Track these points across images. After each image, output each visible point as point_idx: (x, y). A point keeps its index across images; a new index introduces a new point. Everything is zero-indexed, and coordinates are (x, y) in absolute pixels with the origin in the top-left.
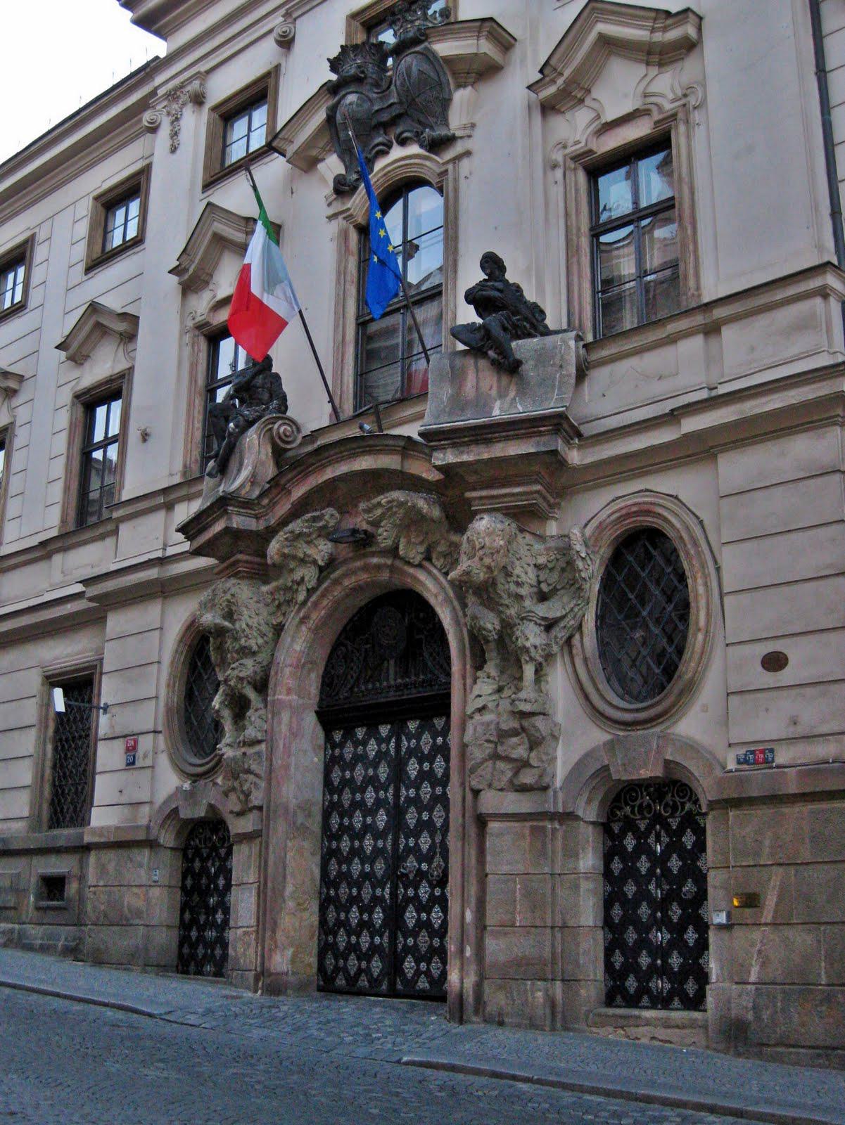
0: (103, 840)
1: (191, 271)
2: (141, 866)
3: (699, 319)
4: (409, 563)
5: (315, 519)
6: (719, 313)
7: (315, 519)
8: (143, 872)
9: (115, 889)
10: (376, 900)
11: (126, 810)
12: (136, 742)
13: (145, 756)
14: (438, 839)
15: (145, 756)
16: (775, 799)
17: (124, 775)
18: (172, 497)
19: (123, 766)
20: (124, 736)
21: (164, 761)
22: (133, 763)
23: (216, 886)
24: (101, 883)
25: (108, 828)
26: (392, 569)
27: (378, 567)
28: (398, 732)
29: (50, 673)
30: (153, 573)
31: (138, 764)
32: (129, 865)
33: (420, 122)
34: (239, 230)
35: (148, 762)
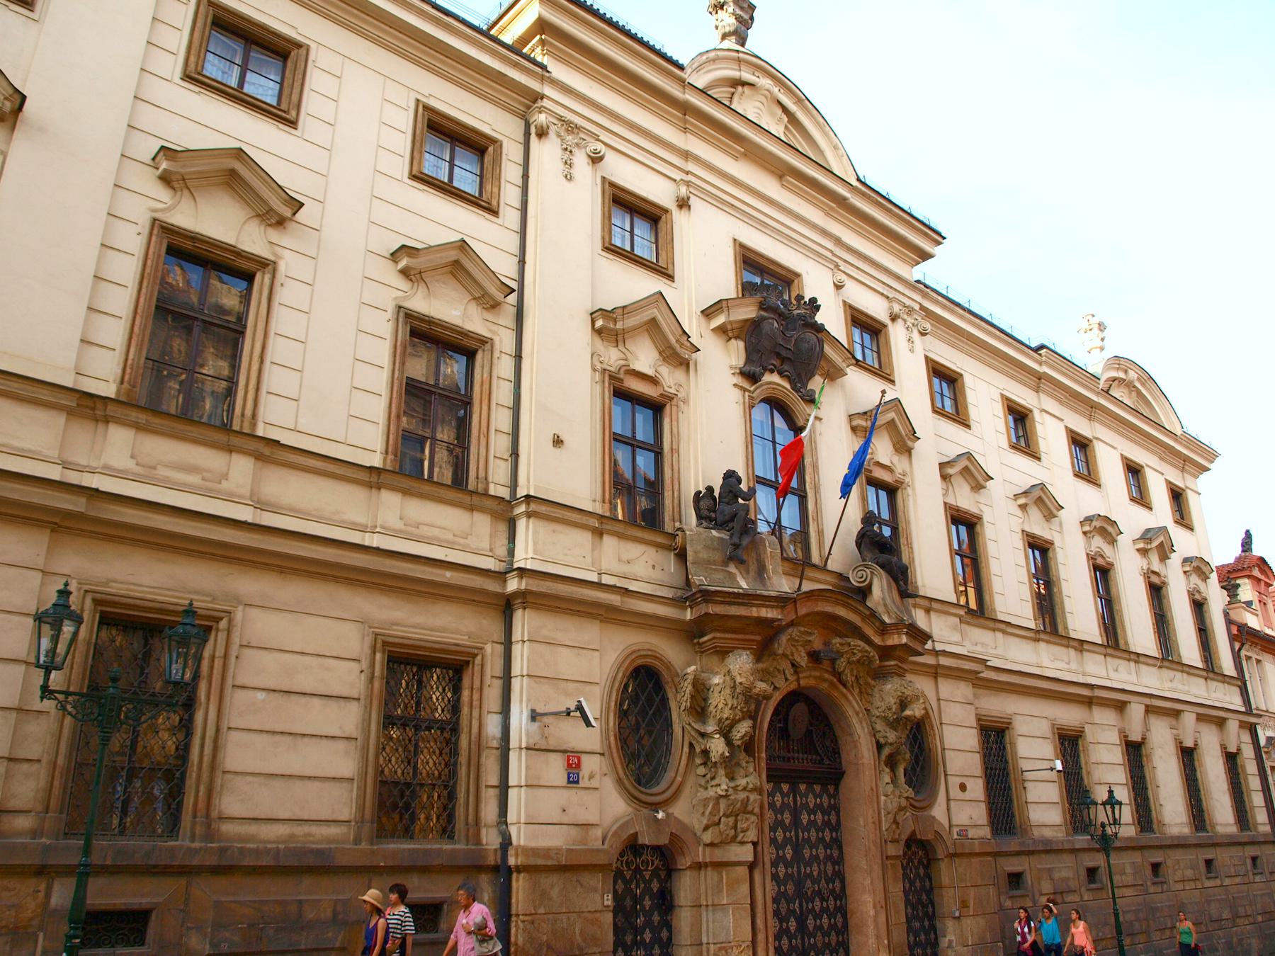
0: (549, 863)
1: (619, 325)
2: (595, 890)
3: (926, 603)
4: (845, 686)
5: (806, 633)
6: (935, 605)
7: (806, 633)
8: (598, 898)
9: (564, 917)
10: (791, 912)
11: (574, 831)
12: (579, 759)
13: (591, 777)
14: (822, 867)
15: (591, 777)
16: (972, 854)
17: (566, 794)
18: (605, 527)
19: (564, 781)
20: (564, 752)
21: (609, 785)
22: (577, 782)
23: (643, 907)
24: (542, 911)
25: (558, 851)
26: (832, 683)
27: (825, 680)
28: (794, 790)
29: (391, 640)
30: (615, 599)
31: (581, 784)
32: (579, 889)
33: (799, 375)
34: (673, 334)
35: (594, 783)
